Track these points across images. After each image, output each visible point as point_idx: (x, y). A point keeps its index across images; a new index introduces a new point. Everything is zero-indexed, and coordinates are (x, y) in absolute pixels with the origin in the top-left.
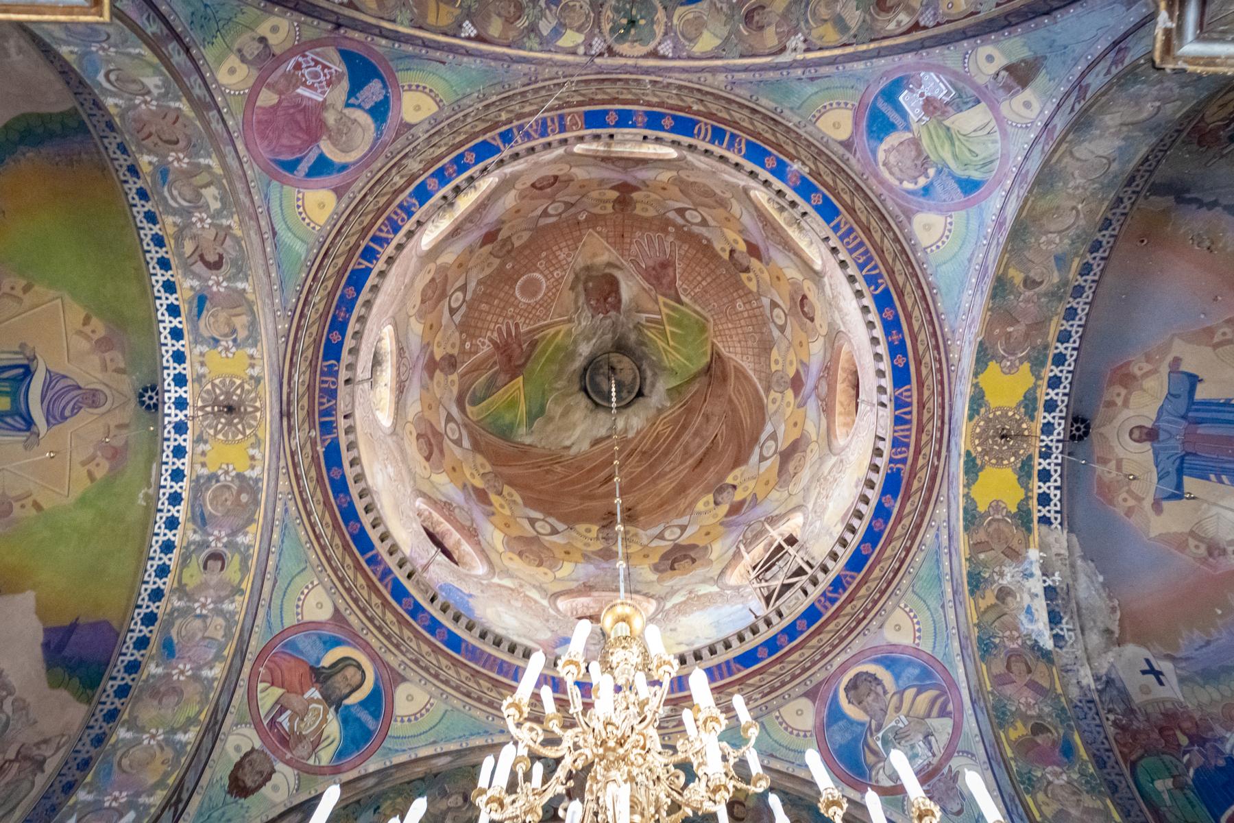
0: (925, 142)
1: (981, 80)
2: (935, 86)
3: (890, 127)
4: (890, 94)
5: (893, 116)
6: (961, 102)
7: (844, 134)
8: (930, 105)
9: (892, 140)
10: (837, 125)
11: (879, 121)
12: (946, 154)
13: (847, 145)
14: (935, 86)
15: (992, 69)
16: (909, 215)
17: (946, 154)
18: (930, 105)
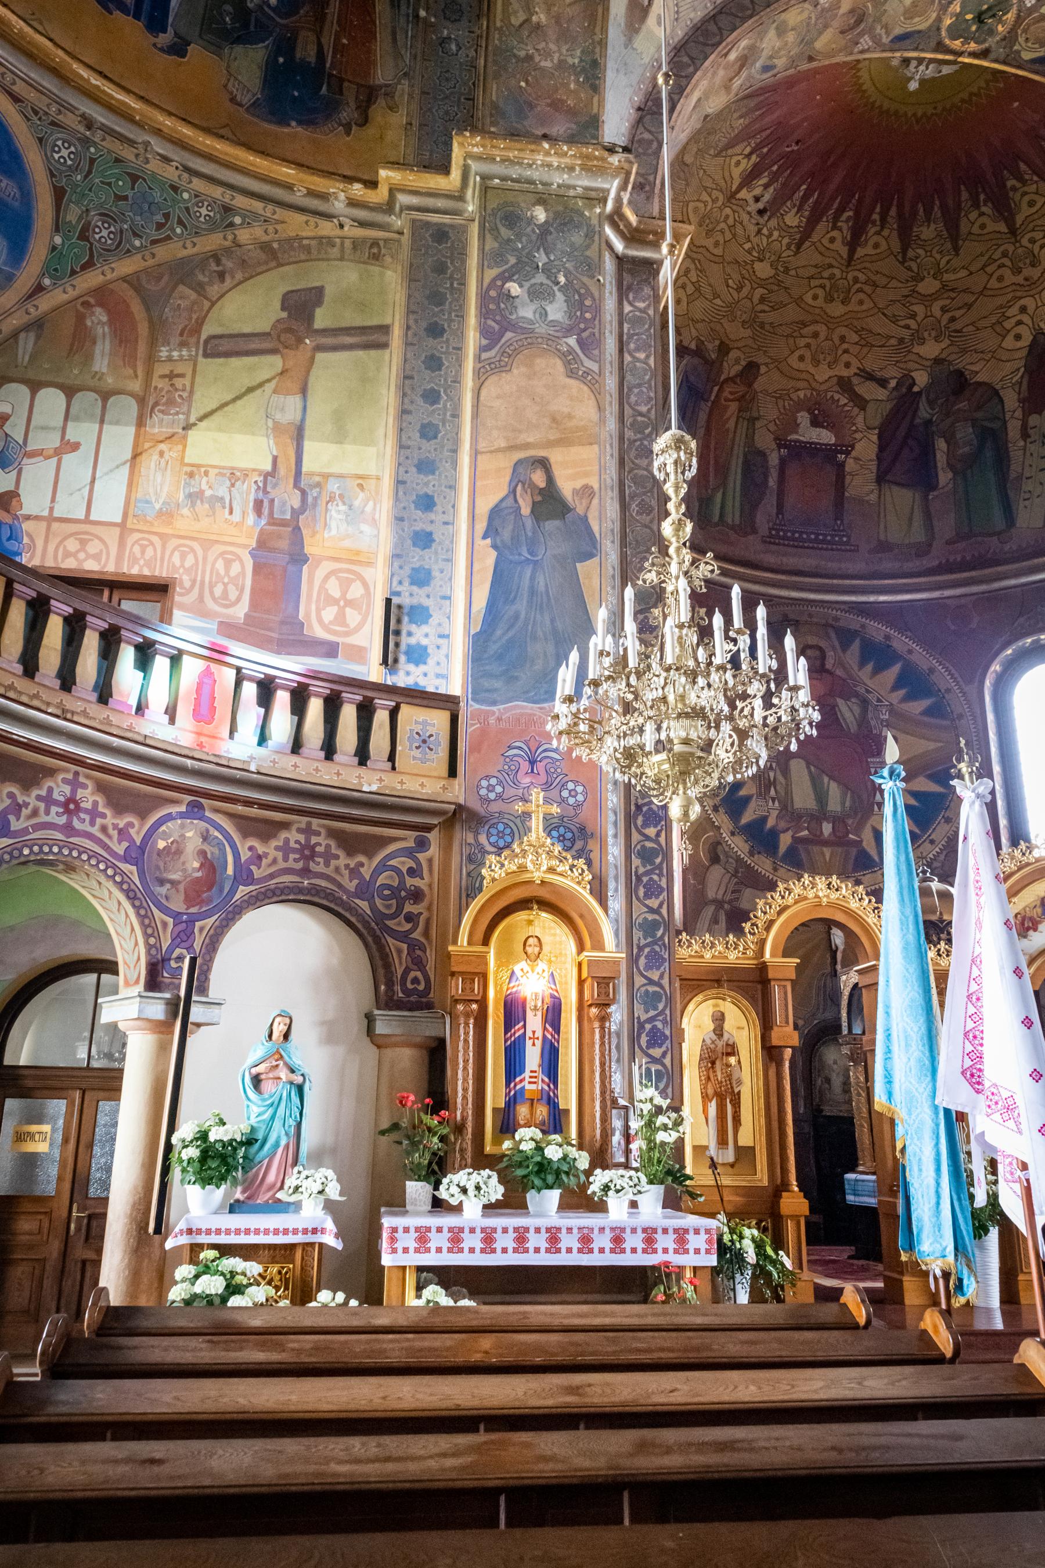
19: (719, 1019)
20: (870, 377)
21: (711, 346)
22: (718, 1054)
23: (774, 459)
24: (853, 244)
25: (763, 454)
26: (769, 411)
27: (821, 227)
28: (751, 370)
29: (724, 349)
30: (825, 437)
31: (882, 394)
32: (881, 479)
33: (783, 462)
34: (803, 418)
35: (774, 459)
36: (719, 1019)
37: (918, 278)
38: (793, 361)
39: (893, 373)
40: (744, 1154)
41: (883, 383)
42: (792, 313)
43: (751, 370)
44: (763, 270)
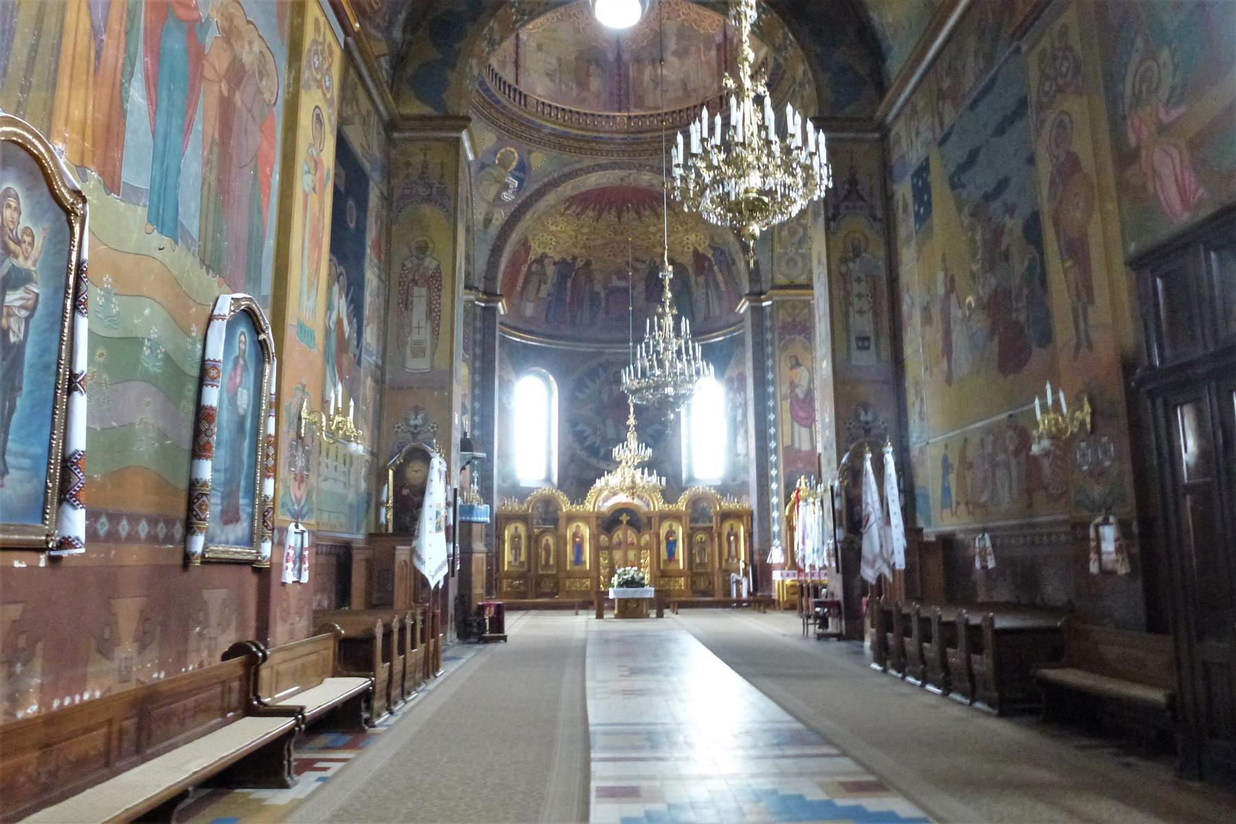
0: (503, 171)
1: (496, 210)
2: (507, 196)
3: (515, 169)
4: (521, 181)
5: (517, 174)
6: (498, 197)
7: (533, 155)
8: (506, 187)
9: (514, 164)
10: (538, 160)
11: (522, 168)
12: (495, 173)
13: (530, 152)
14: (507, 196)
15: (496, 215)
16: (499, 139)
17: (495, 173)
18: (506, 187)
19: (516, 528)
20: (637, 260)
21: (569, 259)
22: (516, 537)
23: (603, 295)
24: (619, 218)
25: (598, 294)
26: (598, 277)
27: (605, 213)
28: (588, 263)
29: (575, 258)
30: (623, 284)
31: (644, 266)
32: (647, 299)
33: (607, 295)
34: (614, 277)
35: (603, 295)
36: (516, 528)
37: (648, 226)
38: (606, 257)
39: (647, 259)
40: (522, 564)
41: (643, 262)
42: (599, 242)
43: (588, 263)
44: (585, 230)
